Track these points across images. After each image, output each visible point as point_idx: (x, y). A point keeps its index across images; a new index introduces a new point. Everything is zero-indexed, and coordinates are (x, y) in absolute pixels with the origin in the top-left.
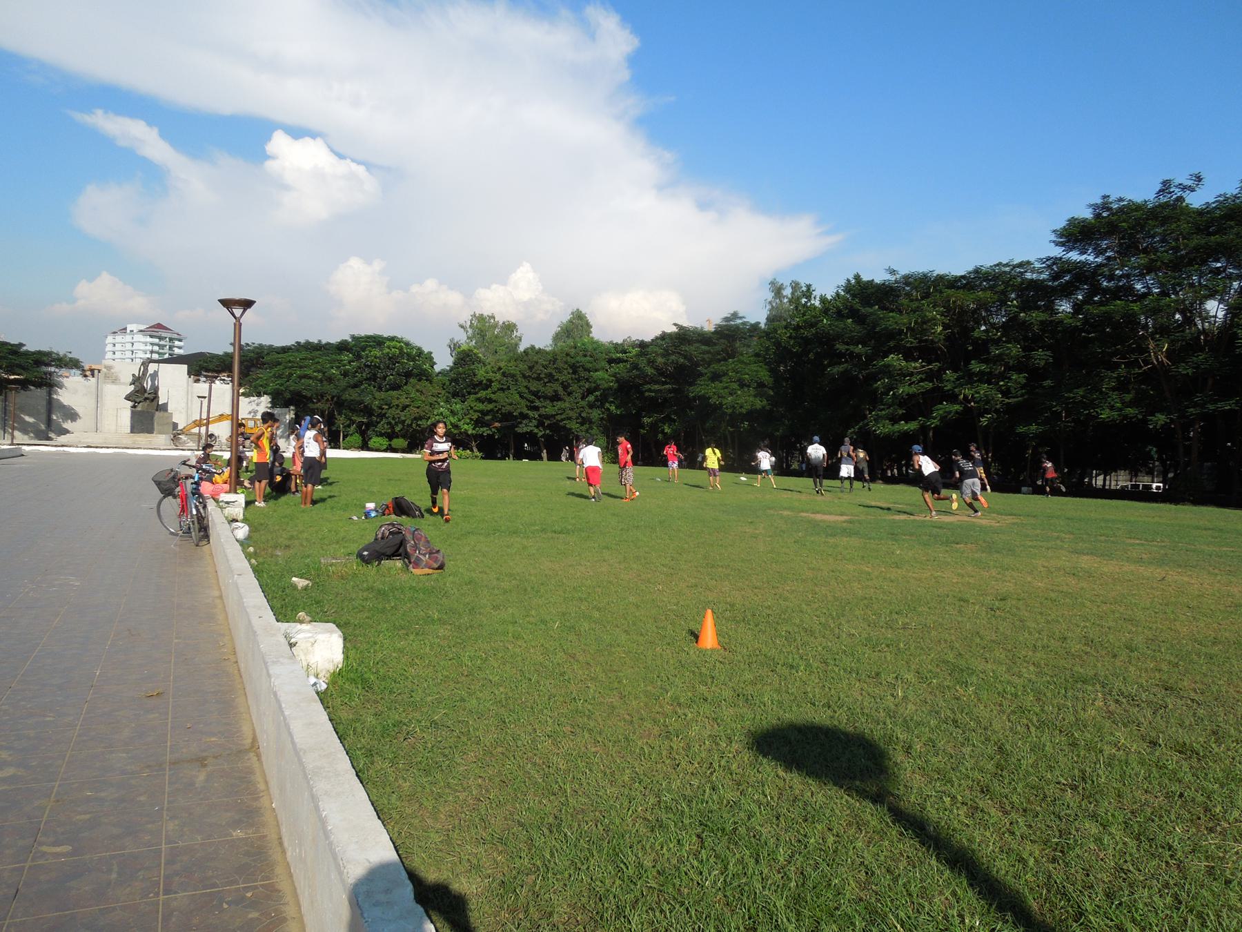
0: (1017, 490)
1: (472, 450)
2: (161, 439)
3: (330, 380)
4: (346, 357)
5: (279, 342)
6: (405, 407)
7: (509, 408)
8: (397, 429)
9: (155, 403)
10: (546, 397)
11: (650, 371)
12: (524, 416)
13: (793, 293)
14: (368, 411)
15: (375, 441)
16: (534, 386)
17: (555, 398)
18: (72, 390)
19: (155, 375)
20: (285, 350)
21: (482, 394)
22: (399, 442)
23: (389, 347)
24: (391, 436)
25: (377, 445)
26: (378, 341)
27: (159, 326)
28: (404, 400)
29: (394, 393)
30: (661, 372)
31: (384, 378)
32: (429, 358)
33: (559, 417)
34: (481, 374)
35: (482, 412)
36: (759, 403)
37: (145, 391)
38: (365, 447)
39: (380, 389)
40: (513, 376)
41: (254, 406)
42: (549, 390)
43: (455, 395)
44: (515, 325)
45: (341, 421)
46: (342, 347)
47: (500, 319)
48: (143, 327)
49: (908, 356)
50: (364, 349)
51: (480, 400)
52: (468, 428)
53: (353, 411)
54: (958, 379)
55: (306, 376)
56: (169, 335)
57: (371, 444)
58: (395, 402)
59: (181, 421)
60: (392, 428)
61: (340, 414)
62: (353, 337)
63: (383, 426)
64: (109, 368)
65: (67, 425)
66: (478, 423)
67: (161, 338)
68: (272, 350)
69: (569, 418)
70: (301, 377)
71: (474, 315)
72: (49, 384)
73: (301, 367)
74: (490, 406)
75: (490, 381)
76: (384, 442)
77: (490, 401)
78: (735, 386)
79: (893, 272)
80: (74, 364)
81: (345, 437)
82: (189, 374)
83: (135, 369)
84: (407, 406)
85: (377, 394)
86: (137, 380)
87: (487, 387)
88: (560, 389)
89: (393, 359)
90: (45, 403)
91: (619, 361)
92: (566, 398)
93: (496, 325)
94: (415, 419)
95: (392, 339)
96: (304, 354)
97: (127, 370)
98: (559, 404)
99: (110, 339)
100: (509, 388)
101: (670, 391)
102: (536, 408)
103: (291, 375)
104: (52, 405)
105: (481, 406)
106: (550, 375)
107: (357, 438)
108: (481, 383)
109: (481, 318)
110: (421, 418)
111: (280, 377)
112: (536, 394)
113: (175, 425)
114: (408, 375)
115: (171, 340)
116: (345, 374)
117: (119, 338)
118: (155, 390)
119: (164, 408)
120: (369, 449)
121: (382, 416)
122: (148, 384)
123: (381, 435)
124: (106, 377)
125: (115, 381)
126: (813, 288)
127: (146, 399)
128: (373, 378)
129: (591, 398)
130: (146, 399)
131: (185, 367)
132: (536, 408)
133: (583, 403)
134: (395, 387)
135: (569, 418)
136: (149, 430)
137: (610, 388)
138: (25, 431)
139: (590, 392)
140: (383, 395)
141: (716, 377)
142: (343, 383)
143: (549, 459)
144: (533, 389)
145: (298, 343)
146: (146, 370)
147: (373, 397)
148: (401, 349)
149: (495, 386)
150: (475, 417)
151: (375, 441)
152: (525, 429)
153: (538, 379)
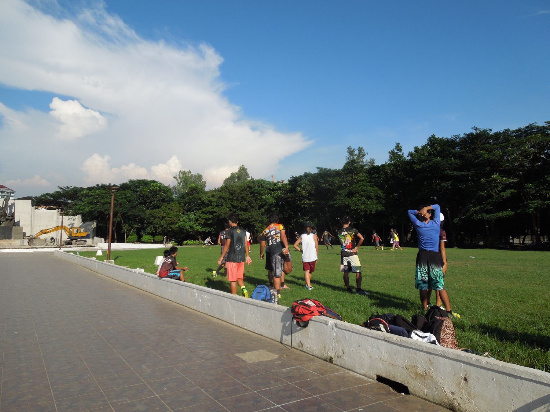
0: (453, 247)
2: (18, 242)
4: (128, 192)
5: (85, 186)
7: (223, 216)
8: (159, 230)
9: (12, 222)
10: (241, 209)
11: (304, 193)
13: (359, 153)
14: (141, 221)
15: (145, 237)
16: (235, 203)
17: (245, 210)
19: (13, 205)
20: (90, 189)
21: (207, 209)
23: (153, 186)
24: (153, 235)
25: (146, 240)
26: (145, 183)
28: (162, 214)
30: (310, 194)
31: (151, 203)
33: (250, 220)
36: (380, 207)
37: (7, 215)
38: (139, 241)
39: (148, 208)
40: (224, 198)
41: (72, 221)
43: (188, 210)
44: (201, 176)
45: (125, 227)
46: (124, 187)
47: (194, 173)
49: (505, 173)
50: (137, 187)
51: (204, 212)
52: (198, 228)
53: (135, 221)
54: (536, 187)
56: (6, 191)
58: (158, 215)
59: (27, 231)
60: (156, 230)
61: (125, 223)
62: (130, 181)
63: (148, 230)
68: (82, 189)
69: (256, 221)
70: (103, 204)
71: (180, 171)
73: (103, 198)
74: (211, 216)
75: (211, 202)
76: (150, 238)
77: (212, 213)
78: (364, 199)
79: (477, 129)
81: (127, 236)
82: (33, 205)
84: (164, 218)
85: (148, 212)
89: (155, 192)
91: (273, 190)
92: (251, 210)
93: (192, 176)
94: (169, 224)
96: (103, 191)
100: (222, 205)
101: (313, 204)
103: (98, 202)
106: (243, 198)
107: (135, 237)
108: (203, 203)
109: (184, 173)
110: (172, 223)
111: (90, 203)
112: (235, 207)
113: (24, 234)
114: (163, 201)
115: (8, 193)
118: (13, 215)
119: (17, 224)
121: (149, 223)
123: (148, 234)
126: (400, 145)
127: (7, 220)
128: (144, 203)
129: (263, 210)
130: (7, 220)
131: (30, 201)
133: (260, 212)
134: (157, 207)
136: (10, 237)
137: (272, 204)
139: (260, 207)
141: (350, 195)
142: (128, 206)
144: (235, 205)
145: (98, 185)
146: (7, 203)
148: (160, 187)
149: (214, 204)
150: (203, 222)
151: (145, 237)
153: (238, 200)
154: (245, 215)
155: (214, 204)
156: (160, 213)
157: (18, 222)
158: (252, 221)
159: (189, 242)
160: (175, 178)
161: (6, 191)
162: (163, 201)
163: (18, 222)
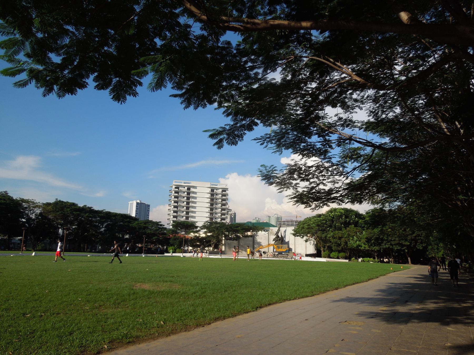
1: (374, 258)
6: (340, 238)
12: (383, 240)
19: (285, 232)
22: (342, 254)
24: (339, 252)
64: (272, 230)
86: (277, 233)
90: (251, 243)
97: (275, 229)
104: (254, 242)
107: (327, 252)
116: (318, 225)
120: (331, 258)
124: (271, 233)
140: (332, 234)
143: (414, 263)
157: (289, 242)
162: (347, 224)
163: (289, 242)
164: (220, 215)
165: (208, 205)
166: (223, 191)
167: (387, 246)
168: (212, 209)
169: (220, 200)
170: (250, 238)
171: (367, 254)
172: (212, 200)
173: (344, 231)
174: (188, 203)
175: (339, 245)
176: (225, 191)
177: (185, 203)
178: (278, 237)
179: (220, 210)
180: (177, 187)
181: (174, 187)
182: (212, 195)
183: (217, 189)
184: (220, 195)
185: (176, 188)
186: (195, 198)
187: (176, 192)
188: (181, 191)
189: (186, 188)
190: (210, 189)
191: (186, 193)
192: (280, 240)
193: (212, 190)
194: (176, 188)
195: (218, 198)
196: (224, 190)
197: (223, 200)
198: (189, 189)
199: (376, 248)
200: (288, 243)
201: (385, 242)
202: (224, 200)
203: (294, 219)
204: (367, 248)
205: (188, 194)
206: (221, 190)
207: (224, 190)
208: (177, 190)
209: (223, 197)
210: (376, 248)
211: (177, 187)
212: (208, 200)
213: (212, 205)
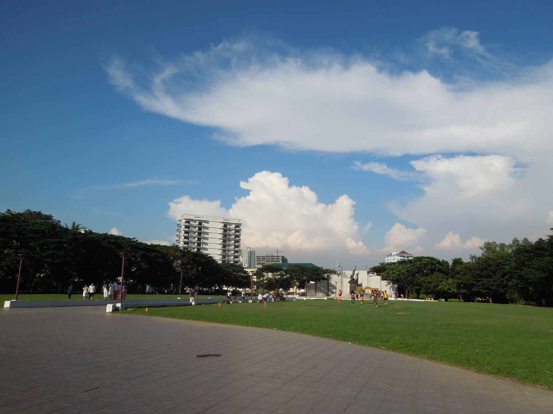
1: (459, 299)
3: (403, 274)
6: (430, 283)
7: (465, 281)
10: (484, 277)
12: (474, 285)
18: (334, 279)
19: (358, 275)
21: (457, 276)
27: (403, 252)
28: (430, 280)
29: (427, 278)
32: (447, 263)
34: (458, 268)
35: (458, 283)
38: (418, 298)
39: (423, 276)
42: (484, 273)
48: (397, 253)
55: (395, 273)
56: (407, 255)
57: (420, 296)
63: (423, 290)
64: (345, 273)
65: (334, 291)
66: (458, 287)
67: (404, 257)
69: (493, 285)
72: (328, 279)
76: (424, 295)
80: (335, 272)
83: (351, 273)
86: (352, 276)
87: (459, 273)
88: (491, 274)
89: (426, 265)
90: (326, 285)
95: (428, 258)
97: (349, 273)
98: (489, 279)
99: (386, 259)
102: (479, 281)
104: (329, 285)
105: (457, 281)
107: (415, 295)
109: (488, 244)
115: (408, 257)
116: (408, 271)
117: (389, 258)
120: (420, 299)
122: (355, 277)
124: (344, 276)
125: (346, 277)
129: (507, 277)
132: (479, 281)
133: (502, 279)
134: (427, 275)
135: (493, 285)
138: (322, 292)
140: (423, 279)
143: (494, 302)
147: (420, 279)
152: (475, 290)
154: (485, 281)
155: (463, 273)
156: (428, 279)
158: (489, 286)
159: (452, 300)
160: (480, 248)
161: (407, 255)
162: (432, 271)
164: (233, 252)
165: (221, 241)
166: (236, 227)
167: (477, 290)
168: (224, 246)
169: (233, 237)
170: (326, 281)
171: (454, 296)
172: (225, 236)
173: (434, 276)
174: (199, 239)
175: (428, 288)
176: (238, 227)
177: (196, 239)
178: (354, 279)
179: (233, 247)
180: (188, 221)
181: (184, 221)
182: (225, 231)
183: (230, 224)
184: (234, 231)
185: (186, 222)
186: (207, 233)
187: (186, 227)
188: (192, 226)
189: (197, 223)
190: (223, 225)
191: (197, 228)
192: (354, 283)
193: (225, 226)
194: (186, 222)
195: (231, 233)
196: (238, 226)
197: (236, 236)
198: (200, 224)
199: (463, 291)
200: (361, 285)
201: (475, 286)
202: (236, 236)
203: (275, 254)
204: (456, 291)
205: (200, 229)
206: (234, 226)
207: (238, 226)
208: (188, 224)
209: (237, 233)
210: (463, 291)
211: (188, 221)
212: (221, 236)
213: (224, 241)
